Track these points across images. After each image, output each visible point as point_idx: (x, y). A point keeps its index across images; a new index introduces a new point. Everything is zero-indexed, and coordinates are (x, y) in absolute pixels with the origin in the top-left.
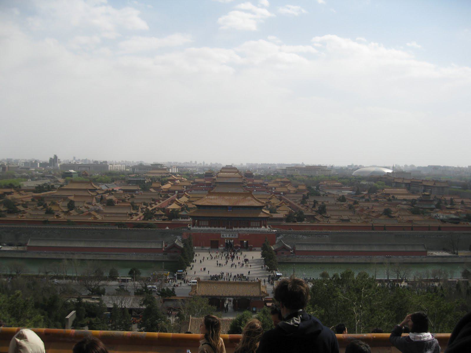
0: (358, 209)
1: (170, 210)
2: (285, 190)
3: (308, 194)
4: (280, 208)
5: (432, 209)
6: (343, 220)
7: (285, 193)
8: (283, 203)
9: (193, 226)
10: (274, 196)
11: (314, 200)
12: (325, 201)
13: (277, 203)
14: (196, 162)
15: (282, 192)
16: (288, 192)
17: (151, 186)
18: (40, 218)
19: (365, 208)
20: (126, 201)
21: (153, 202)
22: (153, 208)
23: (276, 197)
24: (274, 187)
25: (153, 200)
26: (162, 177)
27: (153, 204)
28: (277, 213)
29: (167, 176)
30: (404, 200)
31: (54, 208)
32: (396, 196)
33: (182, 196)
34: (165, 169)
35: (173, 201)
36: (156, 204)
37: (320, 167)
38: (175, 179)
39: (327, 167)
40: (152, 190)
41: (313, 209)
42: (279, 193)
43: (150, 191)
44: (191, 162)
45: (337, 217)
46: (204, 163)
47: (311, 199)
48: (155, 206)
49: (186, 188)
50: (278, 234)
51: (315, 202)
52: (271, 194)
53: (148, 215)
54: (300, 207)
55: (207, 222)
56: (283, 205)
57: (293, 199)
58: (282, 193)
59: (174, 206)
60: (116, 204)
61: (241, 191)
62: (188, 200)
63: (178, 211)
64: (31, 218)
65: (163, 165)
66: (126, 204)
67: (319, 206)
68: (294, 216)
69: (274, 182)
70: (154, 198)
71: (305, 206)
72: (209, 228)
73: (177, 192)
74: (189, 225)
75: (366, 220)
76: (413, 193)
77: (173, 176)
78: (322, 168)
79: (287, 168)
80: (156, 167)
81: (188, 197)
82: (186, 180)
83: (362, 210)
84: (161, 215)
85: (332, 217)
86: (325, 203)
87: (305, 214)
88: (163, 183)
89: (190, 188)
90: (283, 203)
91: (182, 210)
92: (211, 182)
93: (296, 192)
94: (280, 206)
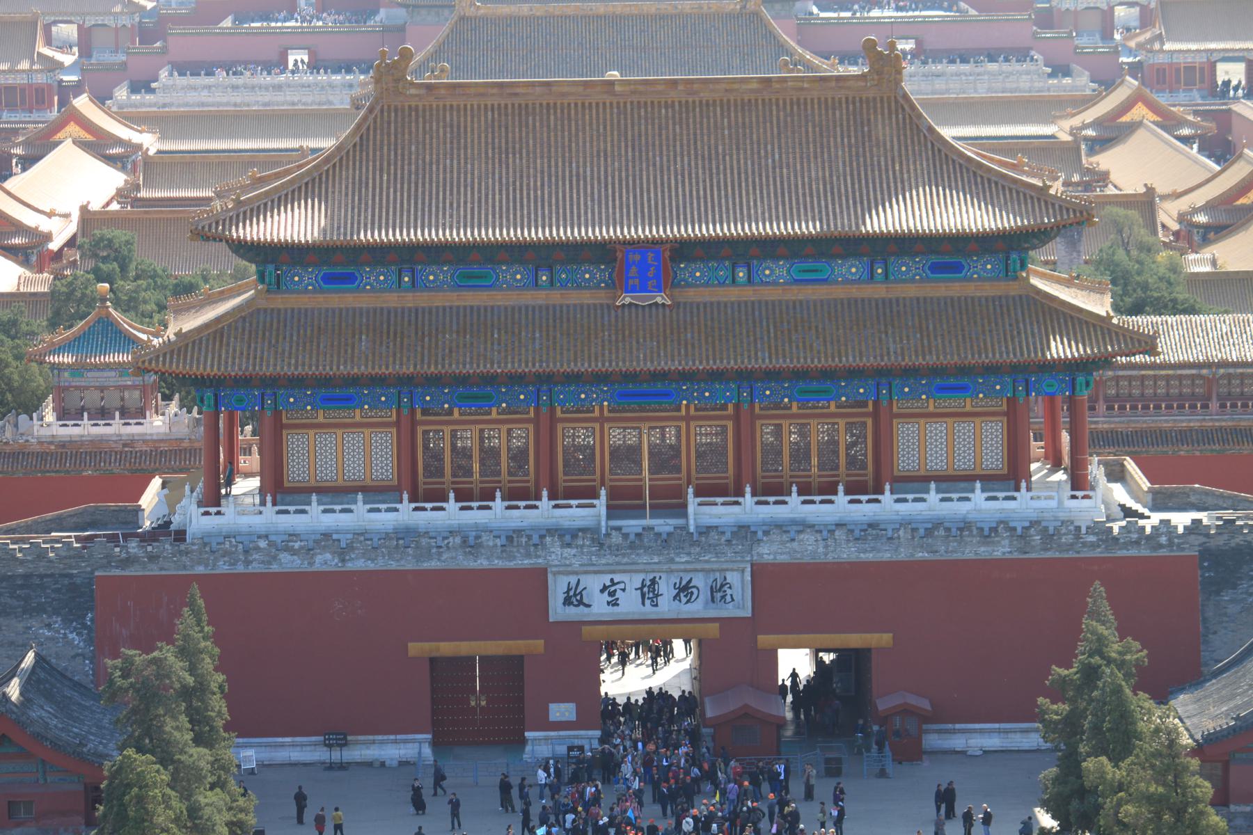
10: (1139, 112)
13: (1177, 195)
52: (1107, 83)
72: (406, 514)
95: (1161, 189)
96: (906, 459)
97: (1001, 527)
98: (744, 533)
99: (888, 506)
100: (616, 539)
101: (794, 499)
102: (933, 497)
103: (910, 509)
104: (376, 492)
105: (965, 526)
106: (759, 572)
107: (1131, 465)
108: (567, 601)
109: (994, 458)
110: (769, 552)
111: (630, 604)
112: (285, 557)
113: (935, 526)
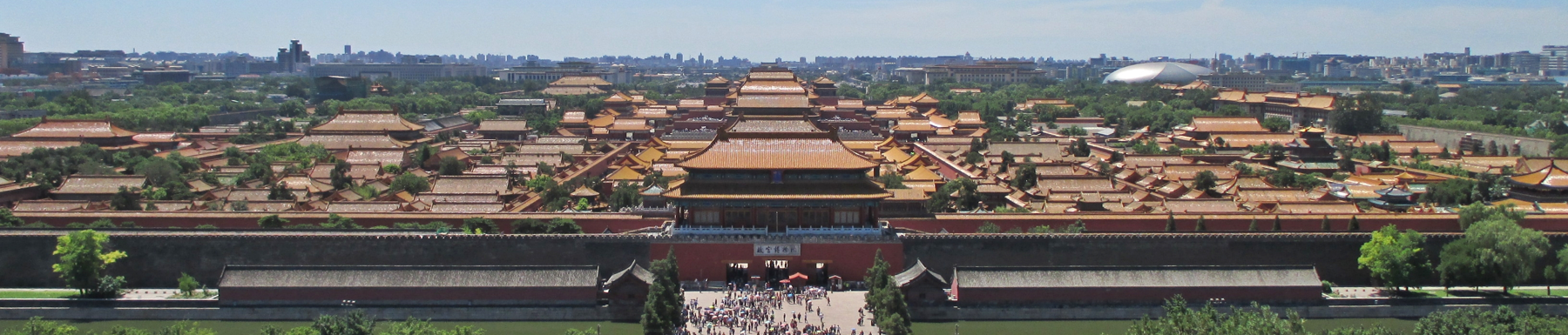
0: (1122, 176)
3: (984, 136)
4: (910, 175)
5: (1328, 173)
7: (923, 136)
14: (680, 56)
18: (255, 211)
19: (1142, 172)
25: (566, 158)
26: (589, 95)
30: (1249, 148)
31: (293, 183)
32: (1226, 139)
36: (575, 170)
40: (564, 132)
41: (1002, 177)
44: (667, 56)
45: (1067, 197)
46: (701, 57)
48: (571, 175)
51: (1008, 159)
61: (806, 127)
63: (635, 187)
64: (228, 213)
66: (494, 171)
72: (721, 230)
73: (629, 135)
75: (1148, 204)
76: (1274, 129)
81: (663, 151)
83: (1134, 178)
84: (591, 199)
85: (1052, 197)
87: (981, 189)
88: (591, 115)
89: (663, 127)
96: (837, 220)
99: (833, 231)
109: (857, 219)
110: (805, 240)
111: (772, 252)
113: (840, 236)
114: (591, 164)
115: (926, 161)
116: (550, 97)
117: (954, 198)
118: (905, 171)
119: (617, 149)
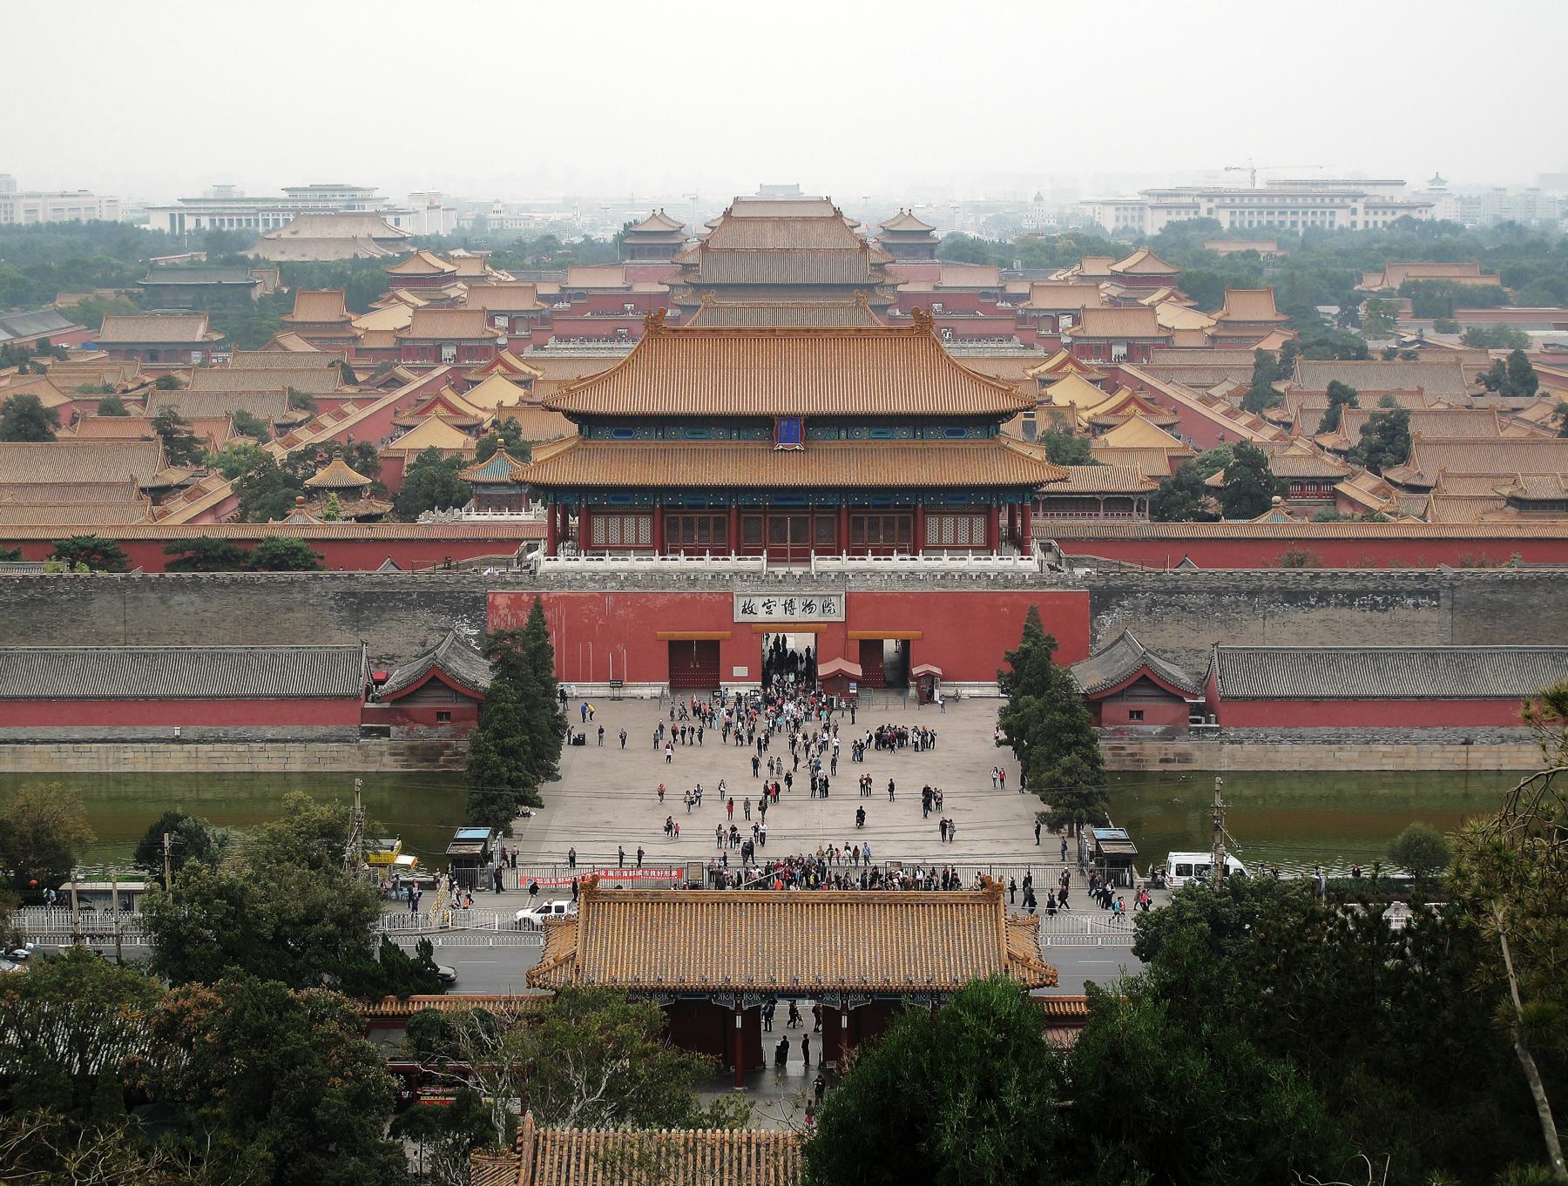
1: (412, 460)
2: (1135, 327)
4: (1113, 439)
6: (1522, 504)
7: (1138, 349)
8: (1133, 407)
9: (552, 552)
10: (1070, 367)
11: (1333, 386)
12: (1400, 392)
13: (1087, 409)
15: (1118, 340)
16: (1167, 340)
17: (288, 319)
20: (127, 413)
21: (300, 416)
22: (299, 448)
23: (1083, 369)
24: (1066, 312)
27: (300, 424)
28: (1095, 463)
29: (387, 260)
33: (487, 371)
34: (377, 217)
35: (424, 406)
37: (1357, 183)
38: (443, 272)
39: (1402, 183)
42: (1101, 348)
43: (284, 348)
47: (1309, 385)
48: (306, 437)
49: (511, 329)
50: (1102, 598)
52: (1051, 354)
53: (269, 490)
54: (1240, 427)
55: (645, 524)
56: (1129, 418)
57: (1194, 381)
58: (1119, 350)
59: (438, 435)
60: (58, 426)
62: (521, 400)
63: (456, 463)
65: (359, 195)
67: (1366, 420)
68: (1207, 482)
69: (1066, 279)
70: (302, 387)
71: (1270, 421)
73: (448, 352)
74: (525, 544)
77: (427, 256)
78: (1369, 190)
79: (1145, 193)
80: (320, 205)
82: (512, 278)
86: (1404, 403)
90: (1133, 407)
91: (485, 452)
92: (667, 289)
93: (1213, 338)
94: (1110, 427)
95: (1079, 405)
96: (932, 538)
97: (982, 575)
98: (841, 574)
99: (922, 563)
100: (772, 578)
101: (870, 558)
102: (946, 558)
103: (933, 564)
104: (640, 549)
105: (964, 574)
106: (849, 598)
107: (1054, 543)
108: (744, 611)
109: (979, 539)
110: (856, 586)
111: (778, 614)
112: (591, 584)
113: (946, 574)
114: (356, 415)
115: (1151, 403)
116: (258, 263)
117: (1210, 490)
118: (1099, 428)
119: (418, 382)
